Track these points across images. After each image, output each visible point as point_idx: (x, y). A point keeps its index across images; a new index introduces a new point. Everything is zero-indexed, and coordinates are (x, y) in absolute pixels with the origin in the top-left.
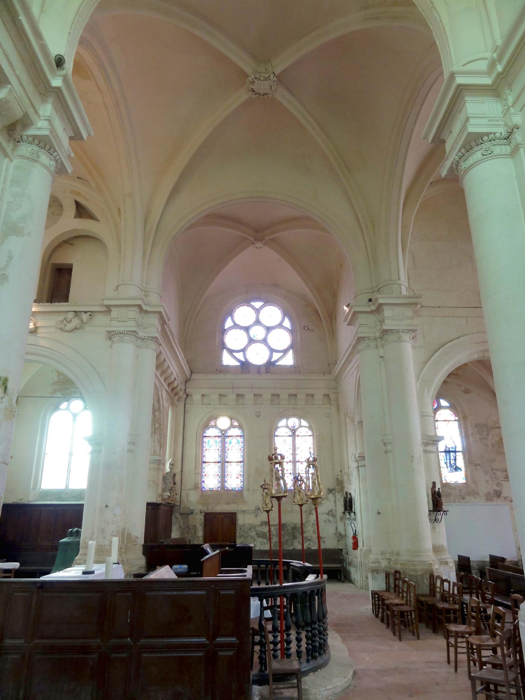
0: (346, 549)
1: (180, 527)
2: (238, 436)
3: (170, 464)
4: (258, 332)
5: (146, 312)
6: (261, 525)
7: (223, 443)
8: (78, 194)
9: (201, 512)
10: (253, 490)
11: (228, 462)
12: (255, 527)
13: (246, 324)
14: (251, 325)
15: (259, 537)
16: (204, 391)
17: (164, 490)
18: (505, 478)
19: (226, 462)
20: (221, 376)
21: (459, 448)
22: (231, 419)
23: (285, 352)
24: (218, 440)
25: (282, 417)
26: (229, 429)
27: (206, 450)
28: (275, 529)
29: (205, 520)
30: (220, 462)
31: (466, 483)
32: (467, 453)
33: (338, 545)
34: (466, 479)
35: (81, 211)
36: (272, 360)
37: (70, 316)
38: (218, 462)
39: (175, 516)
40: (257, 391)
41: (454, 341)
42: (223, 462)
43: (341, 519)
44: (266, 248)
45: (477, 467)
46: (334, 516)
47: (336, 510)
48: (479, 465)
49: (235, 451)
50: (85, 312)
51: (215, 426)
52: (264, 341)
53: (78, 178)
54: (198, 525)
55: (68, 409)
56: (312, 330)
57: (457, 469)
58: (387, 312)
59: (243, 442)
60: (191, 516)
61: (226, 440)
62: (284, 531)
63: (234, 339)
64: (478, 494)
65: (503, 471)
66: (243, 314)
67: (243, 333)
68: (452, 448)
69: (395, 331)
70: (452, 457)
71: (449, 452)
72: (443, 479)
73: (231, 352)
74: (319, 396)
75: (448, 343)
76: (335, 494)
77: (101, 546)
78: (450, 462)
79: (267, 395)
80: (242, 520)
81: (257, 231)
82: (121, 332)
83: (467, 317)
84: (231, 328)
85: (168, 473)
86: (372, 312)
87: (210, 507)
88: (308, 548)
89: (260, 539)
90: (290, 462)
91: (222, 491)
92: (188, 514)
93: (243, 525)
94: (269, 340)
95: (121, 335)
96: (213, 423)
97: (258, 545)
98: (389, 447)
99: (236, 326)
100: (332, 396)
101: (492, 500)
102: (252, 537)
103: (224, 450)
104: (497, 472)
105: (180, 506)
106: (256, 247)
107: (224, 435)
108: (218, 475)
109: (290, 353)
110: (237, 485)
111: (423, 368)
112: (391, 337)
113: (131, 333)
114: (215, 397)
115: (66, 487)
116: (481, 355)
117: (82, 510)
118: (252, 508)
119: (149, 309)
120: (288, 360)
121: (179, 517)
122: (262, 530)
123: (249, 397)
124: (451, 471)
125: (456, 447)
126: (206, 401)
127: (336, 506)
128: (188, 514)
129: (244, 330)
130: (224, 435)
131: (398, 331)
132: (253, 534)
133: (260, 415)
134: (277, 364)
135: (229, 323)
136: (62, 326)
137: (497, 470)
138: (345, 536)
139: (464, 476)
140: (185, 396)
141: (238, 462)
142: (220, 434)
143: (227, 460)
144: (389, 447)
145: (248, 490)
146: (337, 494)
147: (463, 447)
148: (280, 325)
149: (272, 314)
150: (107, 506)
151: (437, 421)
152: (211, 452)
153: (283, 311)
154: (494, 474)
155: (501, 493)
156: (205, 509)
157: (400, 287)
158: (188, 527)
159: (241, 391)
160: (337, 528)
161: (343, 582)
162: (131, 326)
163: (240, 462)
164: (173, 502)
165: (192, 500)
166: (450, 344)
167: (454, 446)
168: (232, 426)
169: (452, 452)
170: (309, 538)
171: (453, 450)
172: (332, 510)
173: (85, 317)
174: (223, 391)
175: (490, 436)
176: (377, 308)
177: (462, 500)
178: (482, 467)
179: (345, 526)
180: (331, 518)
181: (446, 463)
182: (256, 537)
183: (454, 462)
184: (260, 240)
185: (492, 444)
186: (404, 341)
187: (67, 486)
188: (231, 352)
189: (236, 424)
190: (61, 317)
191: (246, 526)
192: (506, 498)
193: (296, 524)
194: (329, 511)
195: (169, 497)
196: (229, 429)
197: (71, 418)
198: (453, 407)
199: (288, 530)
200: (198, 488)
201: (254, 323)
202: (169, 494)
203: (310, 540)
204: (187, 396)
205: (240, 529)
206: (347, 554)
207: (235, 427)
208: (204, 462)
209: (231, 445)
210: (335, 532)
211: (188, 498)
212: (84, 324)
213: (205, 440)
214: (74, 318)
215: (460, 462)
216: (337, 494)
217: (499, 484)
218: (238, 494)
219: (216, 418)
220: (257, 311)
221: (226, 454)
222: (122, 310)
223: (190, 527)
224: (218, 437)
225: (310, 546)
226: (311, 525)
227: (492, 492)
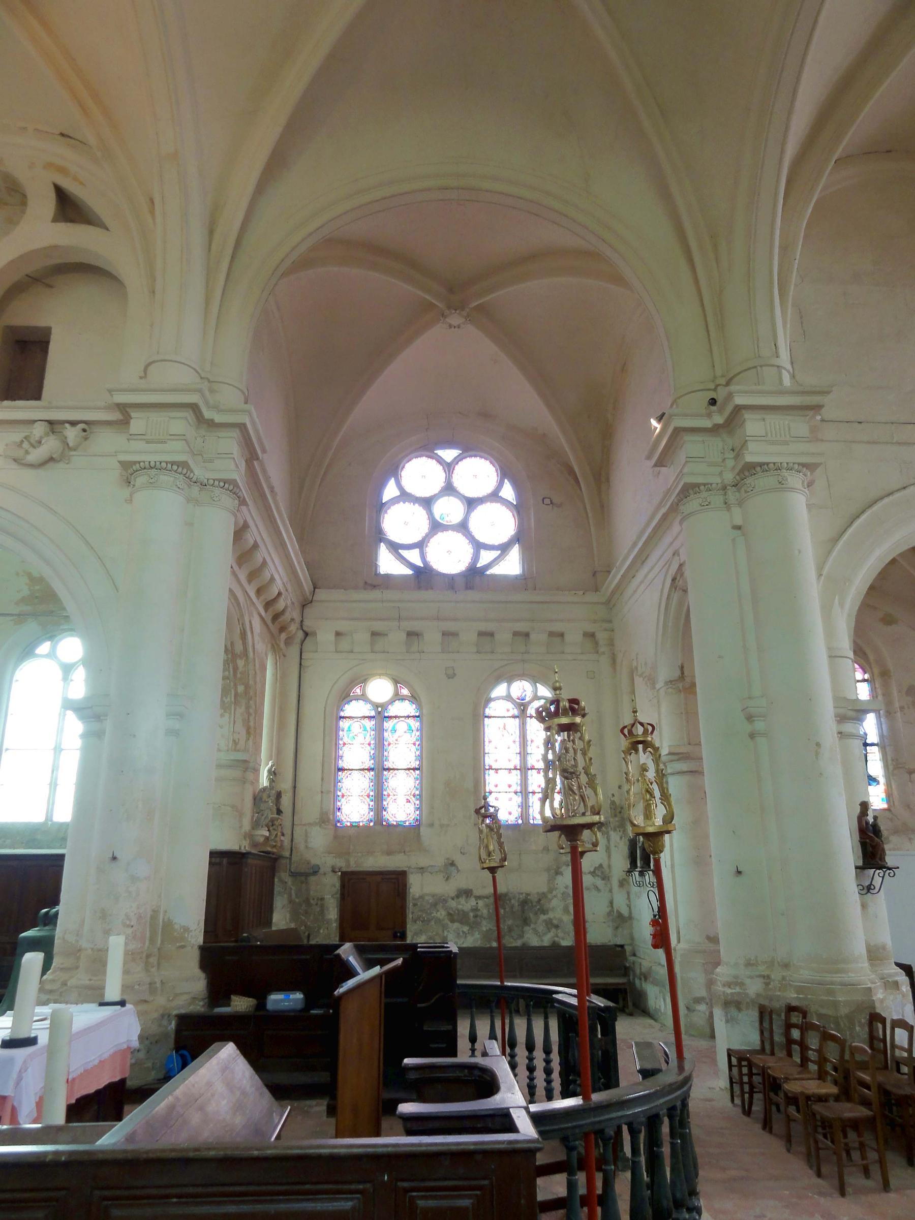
0: (631, 945)
1: (291, 901)
2: (408, 717)
3: (269, 771)
4: (449, 510)
5: (212, 425)
6: (458, 896)
8: (62, 170)
9: (334, 871)
10: (442, 826)
11: (389, 769)
12: (445, 901)
13: (427, 494)
14: (435, 495)
15: (453, 921)
16: (342, 626)
17: (256, 825)
19: (385, 770)
20: (376, 594)
22: (396, 682)
23: (504, 548)
24: (370, 724)
25: (498, 680)
26: (391, 702)
27: (344, 744)
28: (487, 906)
29: (343, 886)
30: (372, 769)
31: (888, 810)
33: (615, 936)
34: (888, 802)
35: (68, 207)
36: (478, 565)
37: (39, 430)
38: (369, 769)
39: (281, 881)
40: (450, 626)
41: (897, 495)
42: (379, 770)
43: (622, 884)
44: (471, 329)
46: (606, 878)
47: (609, 866)
49: (404, 748)
50: (73, 423)
51: (364, 697)
52: (463, 527)
53: (62, 135)
54: (327, 897)
55: (52, 655)
56: (560, 506)
58: (753, 426)
59: (421, 730)
60: (312, 879)
62: (505, 909)
63: (401, 523)
66: (420, 473)
67: (419, 511)
73: (395, 548)
74: (574, 636)
75: (882, 498)
76: (608, 833)
77: (100, 950)
79: (469, 636)
80: (417, 886)
81: (451, 290)
82: (152, 464)
84: (394, 501)
85: (265, 789)
86: (715, 430)
87: (352, 863)
88: (554, 942)
89: (456, 925)
90: (515, 769)
91: (378, 828)
92: (307, 875)
93: (421, 897)
94: (473, 525)
95: (153, 472)
96: (358, 691)
97: (451, 936)
98: (760, 725)
99: (405, 496)
100: (601, 636)
102: (438, 921)
103: (380, 745)
105: (290, 859)
106: (450, 326)
107: (380, 715)
108: (368, 796)
109: (515, 553)
112: (762, 481)
113: (175, 467)
114: (363, 637)
115: (47, 819)
117: (61, 867)
118: (440, 861)
119: (218, 418)
120: (511, 565)
121: (289, 880)
122: (460, 907)
123: (432, 637)
126: (344, 644)
127: (609, 857)
128: (307, 875)
129: (420, 505)
130: (380, 715)
131: (778, 468)
132: (441, 914)
133: (455, 675)
134: (488, 573)
135: (390, 491)
136: (19, 453)
138: (630, 917)
139: (883, 795)
140: (300, 634)
141: (409, 769)
142: (373, 713)
143: (388, 764)
144: (760, 725)
145: (431, 825)
146: (612, 833)
147: (881, 736)
148: (494, 496)
149: (478, 474)
150: (114, 858)
152: (355, 751)
153: (502, 469)
156: (341, 863)
158: (307, 901)
159: (416, 626)
160: (611, 903)
161: (631, 1014)
162: (175, 451)
163: (414, 769)
164: (275, 850)
165: (315, 846)
166: (886, 500)
168: (397, 697)
170: (555, 922)
172: (601, 866)
173: (72, 434)
174: (378, 626)
176: (726, 421)
179: (629, 898)
180: (599, 883)
182: (447, 921)
184: (459, 307)
186: (792, 489)
187: (49, 816)
188: (395, 548)
189: (405, 692)
190: (16, 436)
191: (427, 898)
193: (528, 894)
194: (595, 868)
195: (267, 838)
196: (391, 702)
197: (59, 674)
199: (512, 907)
200: (329, 820)
201: (440, 492)
202: (267, 834)
203: (557, 927)
204: (306, 634)
205: (415, 905)
206: (634, 955)
207: (403, 698)
208: (342, 770)
209: (396, 736)
210: (608, 910)
211: (306, 841)
212: (70, 449)
213: (343, 724)
214: (47, 435)
216: (612, 833)
218: (409, 836)
219: (363, 680)
220: (449, 468)
221: (386, 754)
222: (156, 417)
223: (312, 901)
224: (370, 718)
225: (556, 939)
226: (559, 895)
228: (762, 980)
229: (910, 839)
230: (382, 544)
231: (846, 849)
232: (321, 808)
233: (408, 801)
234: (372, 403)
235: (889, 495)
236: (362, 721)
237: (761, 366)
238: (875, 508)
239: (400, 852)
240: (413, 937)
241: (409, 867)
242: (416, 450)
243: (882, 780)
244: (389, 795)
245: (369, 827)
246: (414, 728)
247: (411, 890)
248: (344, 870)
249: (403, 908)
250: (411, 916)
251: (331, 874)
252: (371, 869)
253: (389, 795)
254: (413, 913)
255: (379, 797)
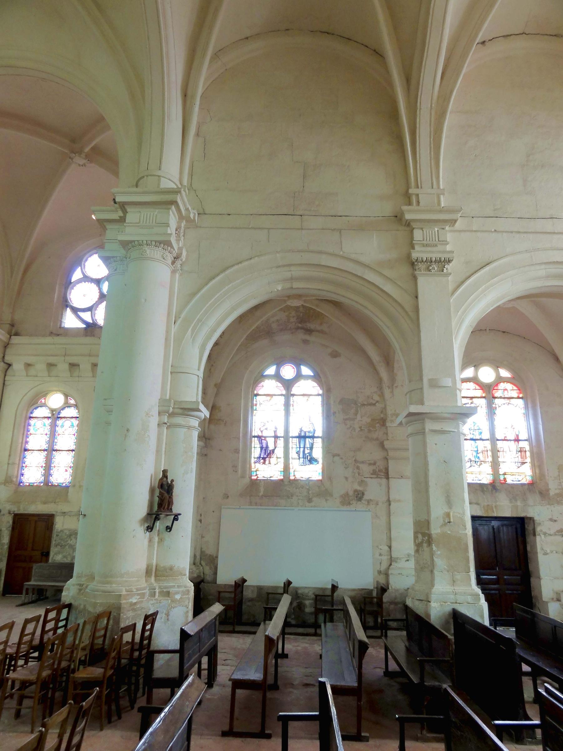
2: (72, 417)
7: (53, 426)
9: (9, 513)
11: (57, 450)
13: (99, 277)
16: (30, 360)
18: (372, 474)
20: (57, 340)
21: (319, 433)
22: (66, 396)
29: (14, 522)
31: (321, 481)
32: (328, 438)
38: (44, 450)
42: (50, 451)
45: (336, 458)
48: (339, 455)
54: (4, 529)
57: (312, 460)
58: (132, 216)
64: (331, 495)
65: (370, 464)
67: (93, 287)
68: (309, 432)
69: (136, 243)
70: (308, 445)
71: (305, 437)
72: (292, 475)
73: (75, 311)
75: (233, 266)
78: (304, 451)
80: (60, 524)
81: (73, 141)
83: (269, 229)
84: (79, 281)
87: (21, 508)
93: (62, 531)
99: (86, 278)
101: (349, 504)
103: (53, 434)
104: (361, 466)
106: (79, 165)
107: (55, 416)
111: (188, 302)
114: (41, 367)
116: (288, 285)
123: (85, 366)
124: (304, 464)
125: (314, 431)
126: (32, 371)
130: (55, 416)
135: (77, 275)
137: (363, 462)
141: (69, 450)
142: (50, 415)
143: (56, 447)
145: (74, 486)
147: (323, 432)
151: (293, 395)
152: (37, 438)
154: (358, 468)
155: (363, 494)
156: (15, 509)
157: (159, 181)
159: (74, 360)
167: (312, 430)
169: (309, 437)
171: (311, 435)
174: (52, 360)
175: (359, 417)
177: (307, 504)
178: (342, 458)
181: (298, 453)
183: (309, 451)
184: (79, 152)
185: (360, 427)
188: (75, 311)
189: (72, 402)
192: (369, 502)
198: (317, 378)
200: (12, 481)
205: (57, 536)
209: (63, 429)
215: (318, 453)
217: (362, 483)
218: (62, 492)
219: (45, 394)
221: (56, 441)
224: (48, 418)
227: (351, 493)
228: (78, 587)
229: (326, 500)
230: (68, 309)
231: (139, 501)
232: (7, 474)
233: (66, 471)
234: (50, 216)
235: (238, 264)
237: (147, 176)
238: (228, 272)
239: (52, 502)
240: (53, 556)
241: (57, 512)
242: (95, 248)
243: (320, 461)
245: (40, 486)
246: (75, 425)
247: (56, 526)
248: (16, 512)
249: (50, 538)
250: (54, 542)
251: (8, 515)
252: (32, 513)
253: (55, 467)
254: (55, 541)
255: (48, 468)
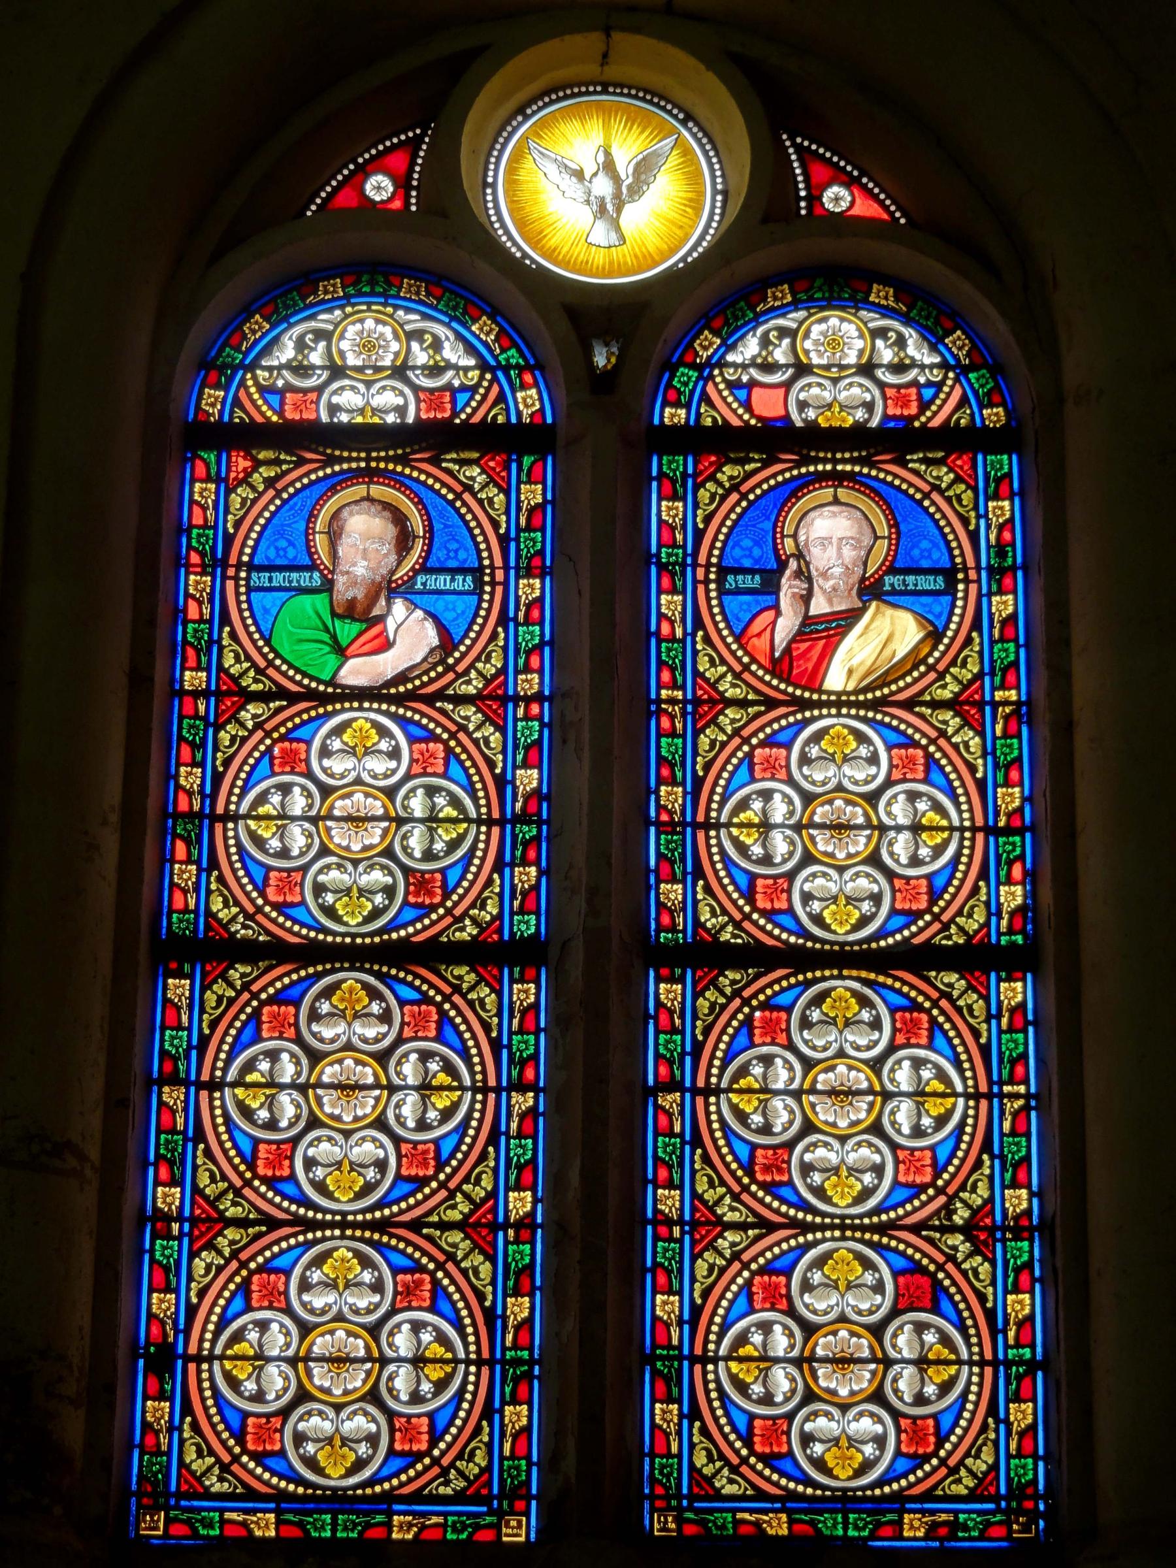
24: (495, 502)
38: (492, 955)
42: (600, 958)
49: (856, 776)
59: (1044, 561)
61: (665, 510)
108: (483, 1227)
110: (921, 1436)
141: (920, 959)
168: (768, 257)
207: (834, 279)
213: (225, 501)
224: (498, 441)
233: (920, 1290)
236: (421, 472)
244: (703, 1225)
253: (703, 1225)
